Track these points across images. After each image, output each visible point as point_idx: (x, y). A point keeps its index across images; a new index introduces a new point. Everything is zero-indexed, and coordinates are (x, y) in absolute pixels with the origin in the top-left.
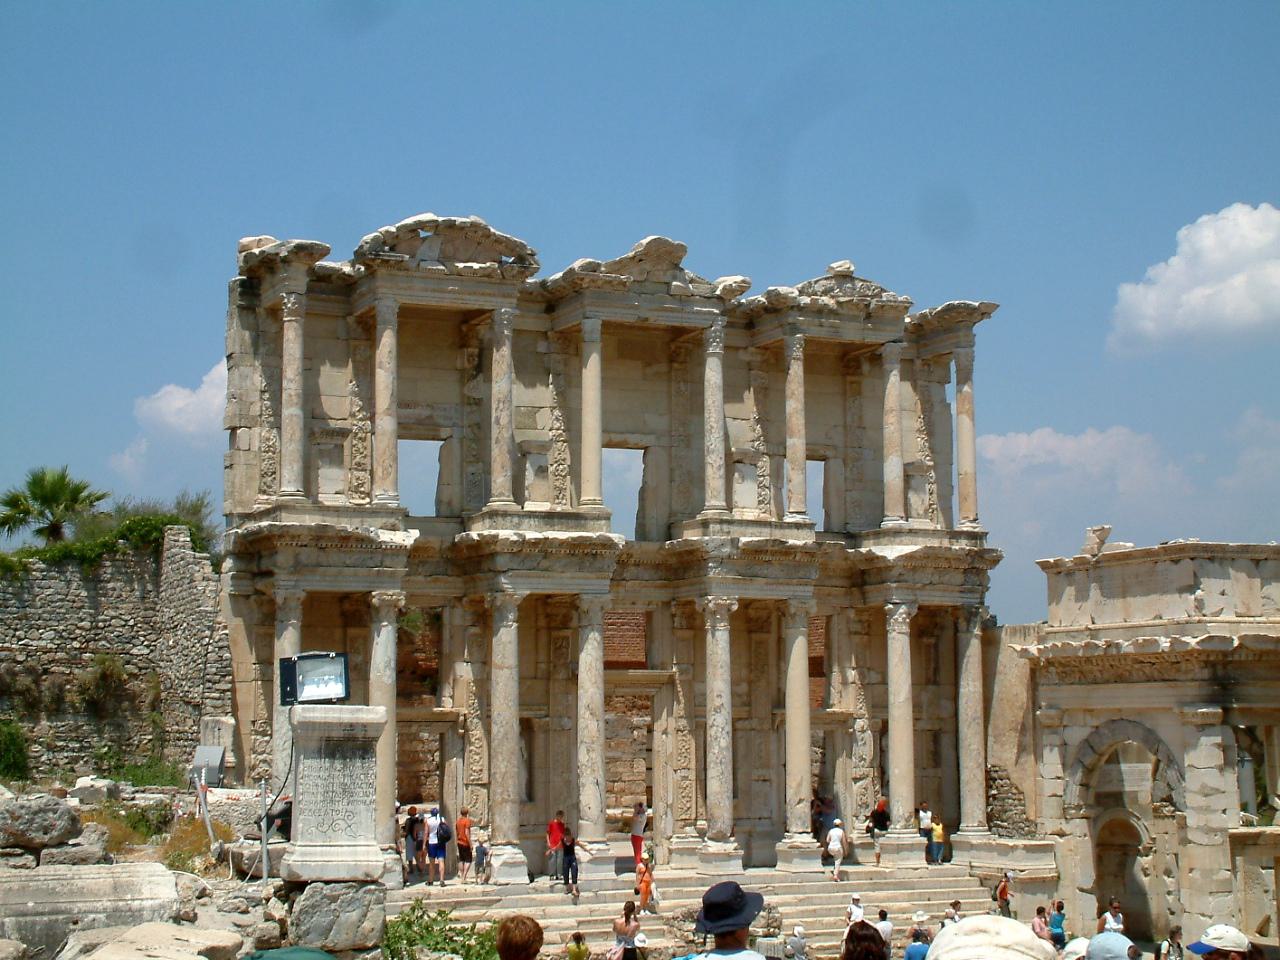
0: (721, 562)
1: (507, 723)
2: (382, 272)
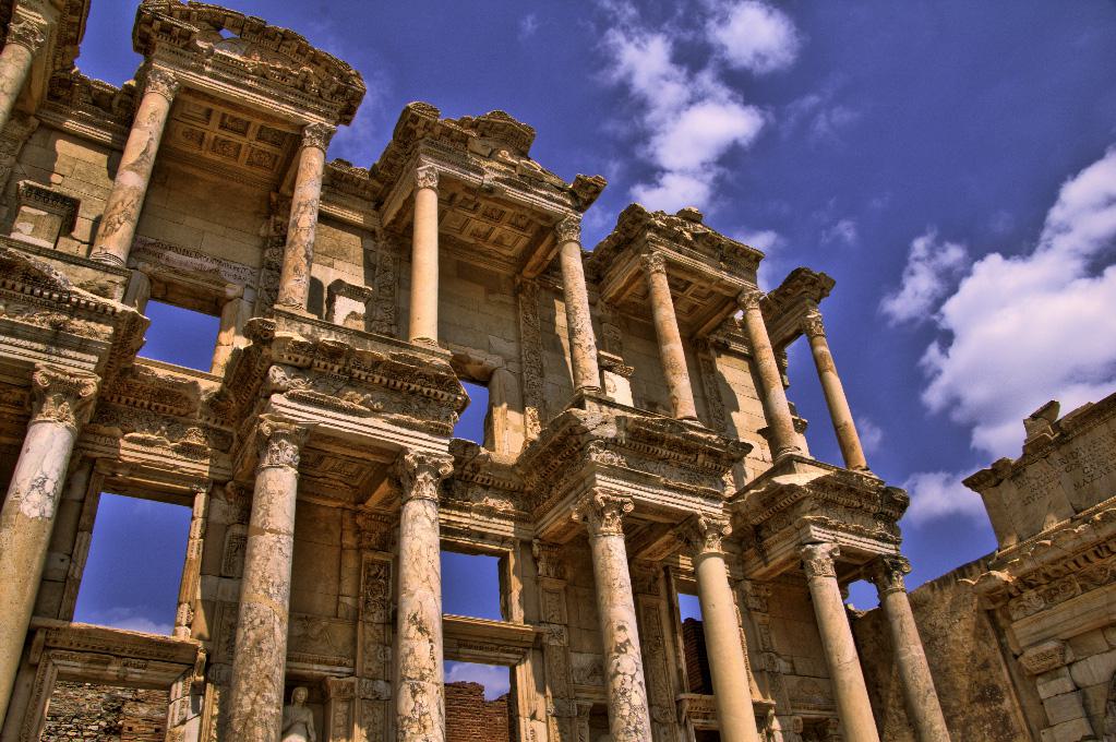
0: (609, 444)
1: (262, 622)
2: (161, 43)
